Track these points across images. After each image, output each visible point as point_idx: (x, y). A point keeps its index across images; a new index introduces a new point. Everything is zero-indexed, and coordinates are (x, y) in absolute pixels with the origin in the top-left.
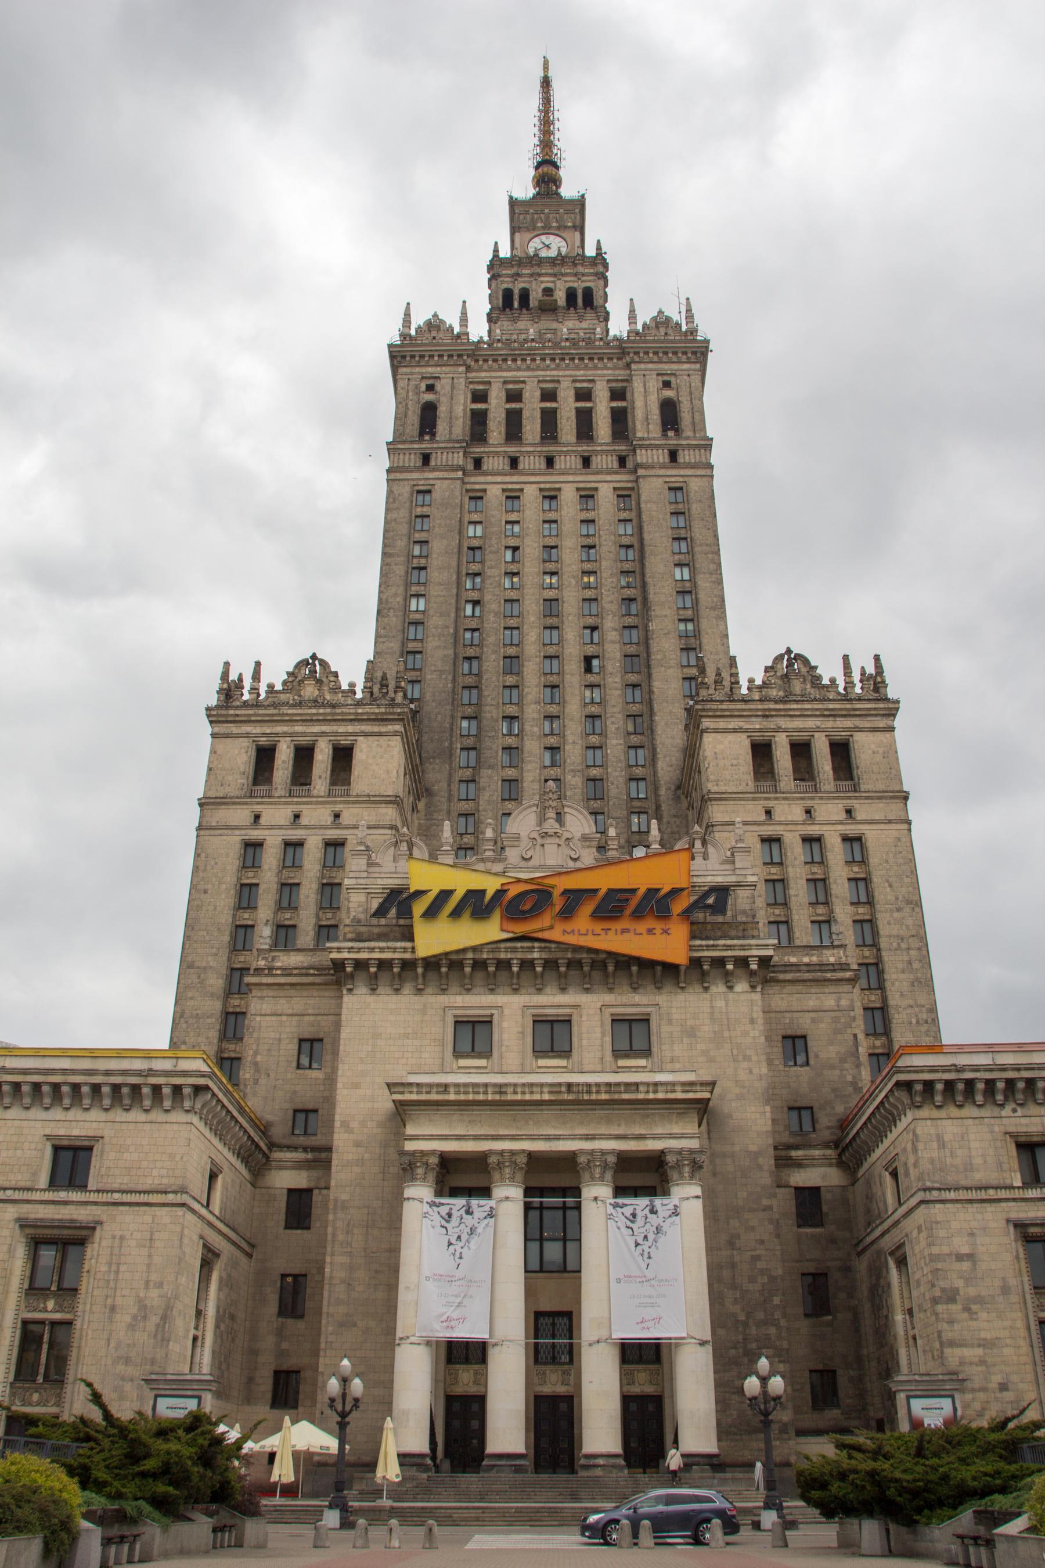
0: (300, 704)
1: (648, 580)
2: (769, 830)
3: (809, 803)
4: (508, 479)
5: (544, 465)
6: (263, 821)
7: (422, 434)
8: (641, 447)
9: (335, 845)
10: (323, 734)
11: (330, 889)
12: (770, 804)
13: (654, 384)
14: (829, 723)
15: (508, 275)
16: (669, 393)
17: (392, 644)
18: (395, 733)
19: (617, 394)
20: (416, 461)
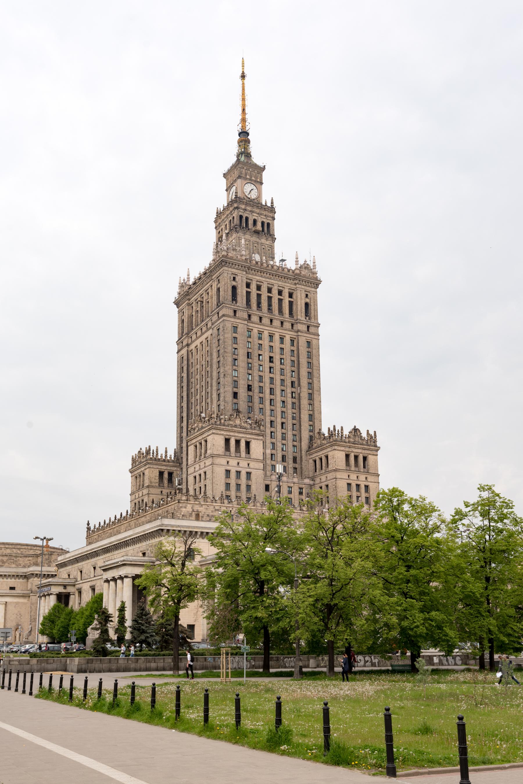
0: (236, 426)
1: (301, 377)
2: (349, 482)
3: (358, 475)
4: (259, 326)
5: (270, 323)
6: (229, 463)
7: (233, 300)
8: (300, 323)
9: (249, 474)
10: (243, 437)
11: (249, 487)
12: (349, 474)
13: (304, 296)
14: (363, 451)
15: (242, 209)
16: (308, 300)
17: (229, 389)
18: (262, 440)
19: (291, 295)
20: (232, 314)
